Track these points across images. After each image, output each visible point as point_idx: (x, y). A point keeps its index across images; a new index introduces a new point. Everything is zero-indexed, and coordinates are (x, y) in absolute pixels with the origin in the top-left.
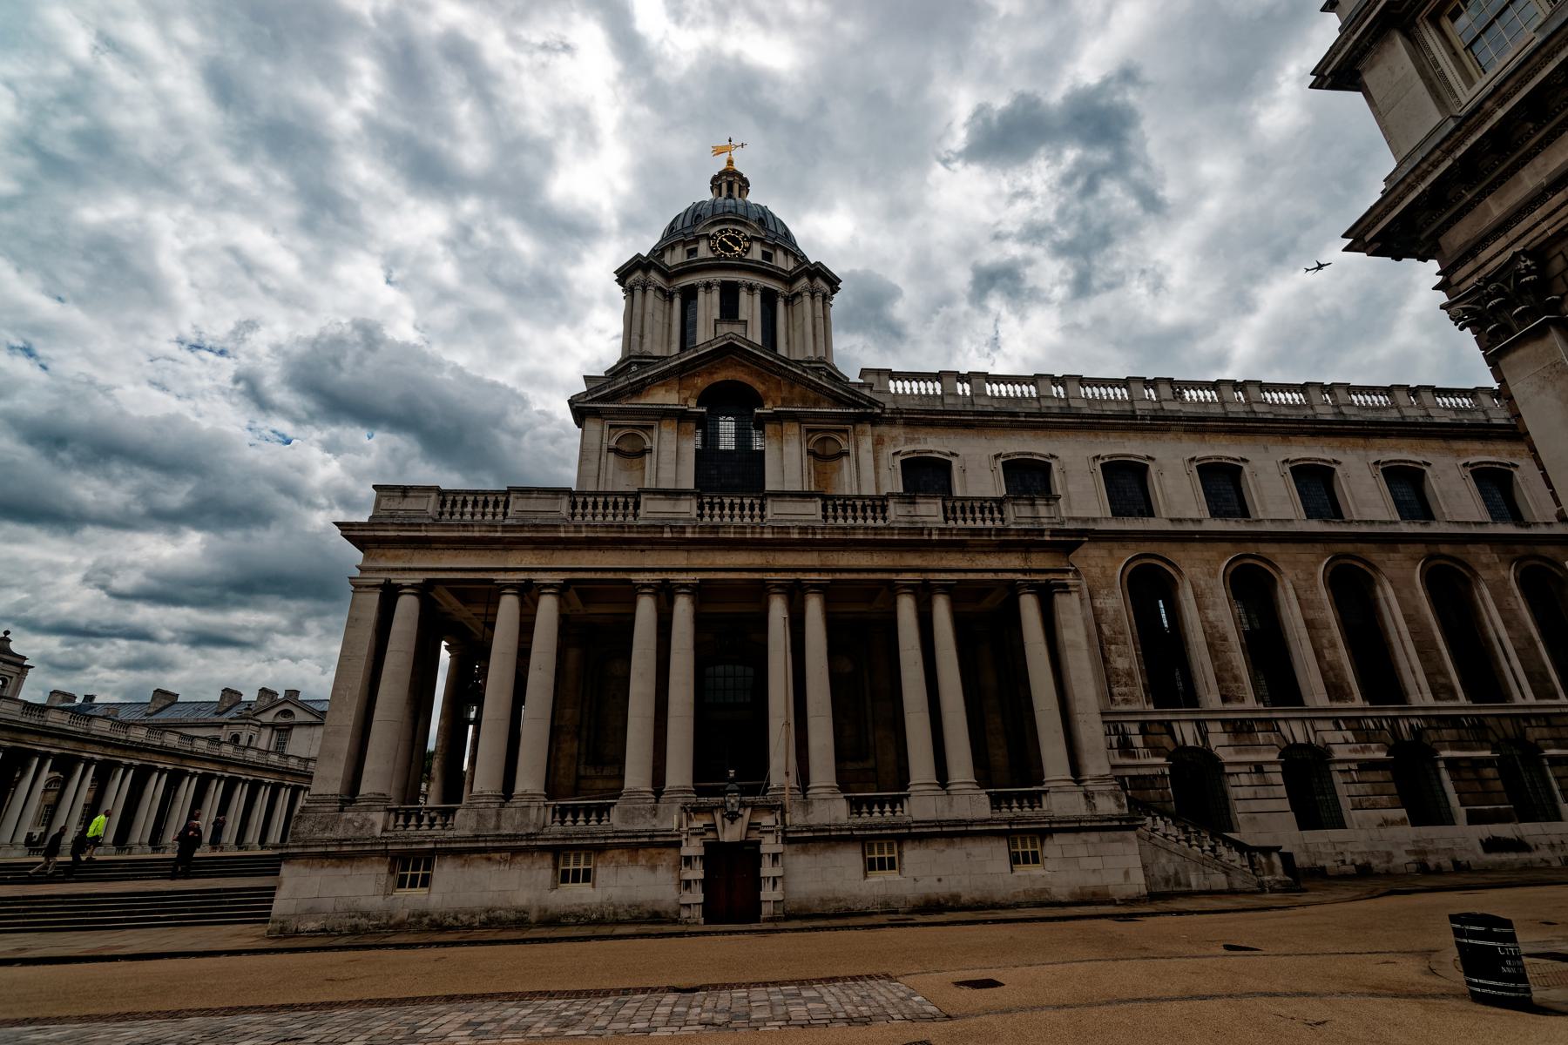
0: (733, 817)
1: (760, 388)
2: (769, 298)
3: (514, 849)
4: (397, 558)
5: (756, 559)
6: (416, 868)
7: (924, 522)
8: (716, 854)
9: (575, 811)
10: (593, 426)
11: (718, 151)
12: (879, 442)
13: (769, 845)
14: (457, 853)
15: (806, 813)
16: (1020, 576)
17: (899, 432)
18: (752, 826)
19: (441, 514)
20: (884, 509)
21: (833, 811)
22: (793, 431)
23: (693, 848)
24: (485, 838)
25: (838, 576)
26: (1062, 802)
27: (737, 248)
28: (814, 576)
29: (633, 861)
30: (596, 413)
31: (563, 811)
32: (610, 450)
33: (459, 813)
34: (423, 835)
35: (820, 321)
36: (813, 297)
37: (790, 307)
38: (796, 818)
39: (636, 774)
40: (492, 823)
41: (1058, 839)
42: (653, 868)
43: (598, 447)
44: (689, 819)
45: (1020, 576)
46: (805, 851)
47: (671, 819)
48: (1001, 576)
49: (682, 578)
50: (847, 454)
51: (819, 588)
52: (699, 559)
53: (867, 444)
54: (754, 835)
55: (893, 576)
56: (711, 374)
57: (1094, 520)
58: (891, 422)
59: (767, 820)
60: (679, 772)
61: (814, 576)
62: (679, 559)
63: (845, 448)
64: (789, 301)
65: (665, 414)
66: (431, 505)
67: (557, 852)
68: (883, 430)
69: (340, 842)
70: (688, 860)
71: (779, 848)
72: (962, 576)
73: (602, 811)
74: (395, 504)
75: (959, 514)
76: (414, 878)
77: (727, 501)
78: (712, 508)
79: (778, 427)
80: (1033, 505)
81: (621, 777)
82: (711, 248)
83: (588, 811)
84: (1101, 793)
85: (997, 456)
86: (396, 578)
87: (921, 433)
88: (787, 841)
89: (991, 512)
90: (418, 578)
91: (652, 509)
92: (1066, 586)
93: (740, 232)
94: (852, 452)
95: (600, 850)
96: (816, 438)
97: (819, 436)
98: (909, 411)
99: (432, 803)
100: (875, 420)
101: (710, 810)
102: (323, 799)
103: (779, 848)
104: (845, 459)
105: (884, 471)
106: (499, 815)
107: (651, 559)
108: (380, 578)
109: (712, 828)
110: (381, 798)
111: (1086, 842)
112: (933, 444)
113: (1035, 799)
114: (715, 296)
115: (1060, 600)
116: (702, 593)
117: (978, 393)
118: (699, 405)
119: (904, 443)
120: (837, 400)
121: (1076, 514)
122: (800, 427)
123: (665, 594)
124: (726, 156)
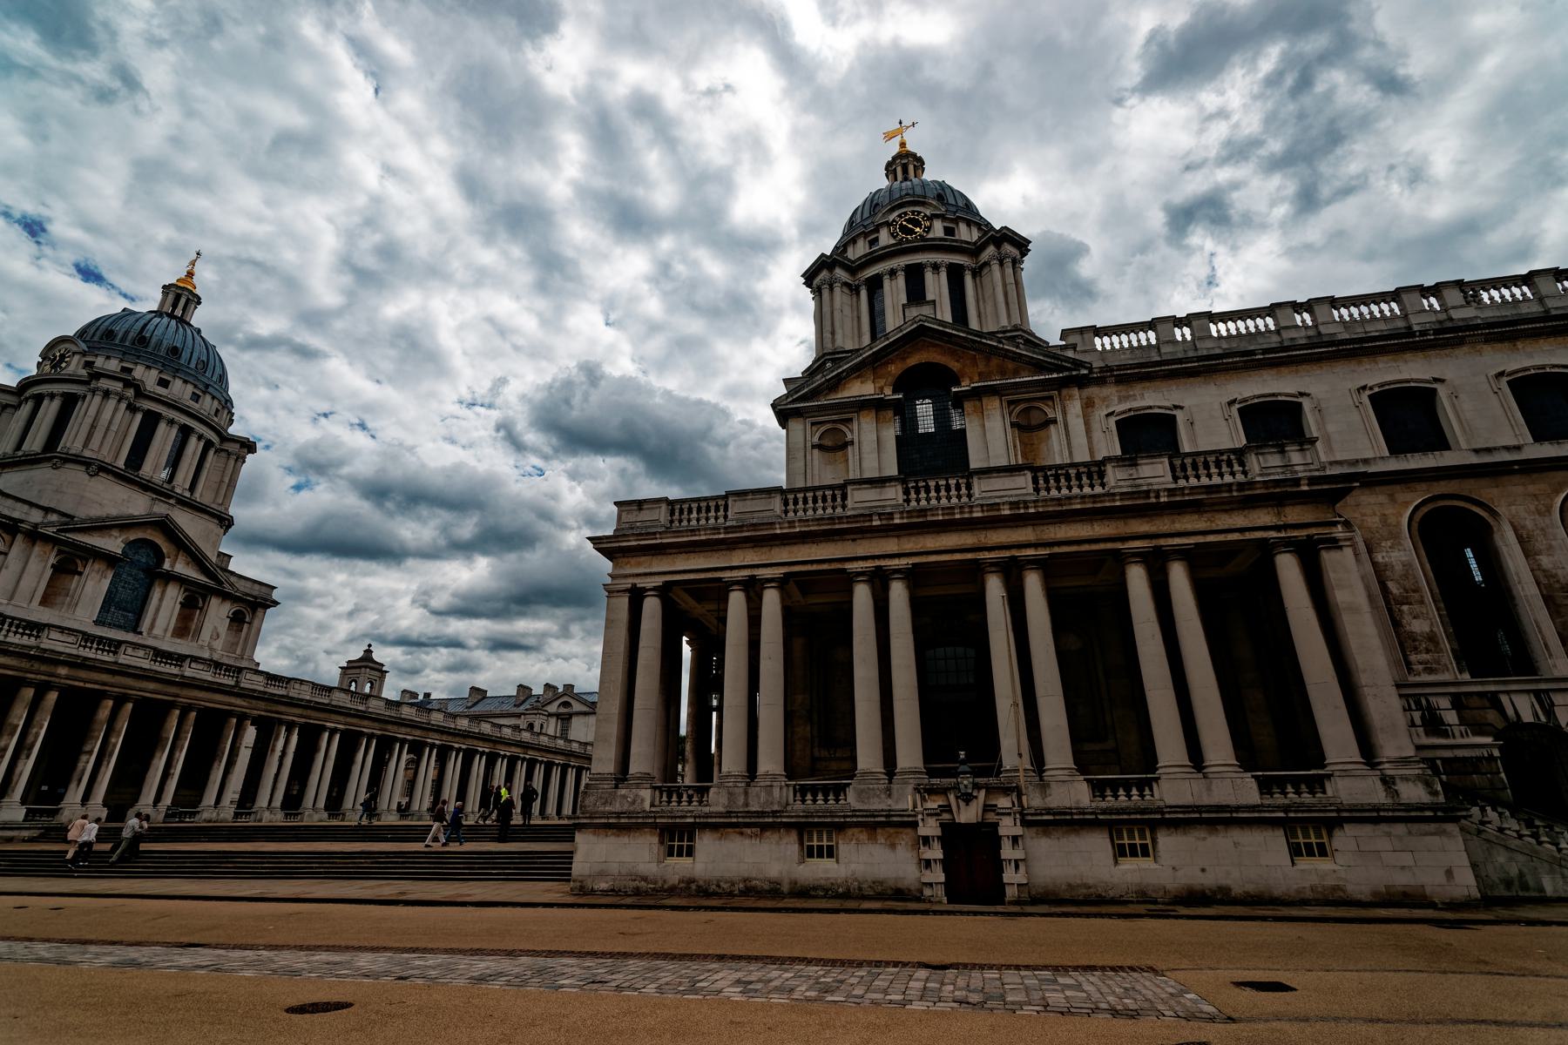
0: (968, 799)
1: (955, 366)
2: (955, 274)
3: (763, 824)
4: (639, 564)
5: (967, 539)
6: (681, 840)
7: (1151, 484)
8: (952, 834)
9: (814, 790)
10: (797, 425)
11: (889, 136)
12: (1088, 405)
13: (1008, 827)
14: (715, 827)
15: (1044, 794)
16: (1273, 534)
17: (1110, 391)
18: (987, 808)
19: (672, 522)
20: (1102, 475)
21: (1076, 794)
22: (994, 407)
23: (930, 828)
25: (1056, 550)
27: (918, 229)
28: (1030, 552)
29: (873, 838)
30: (798, 413)
31: (802, 791)
32: (813, 447)
33: (712, 790)
34: (686, 809)
35: (1012, 289)
36: (1001, 264)
37: (978, 279)
38: (1034, 800)
39: (868, 756)
40: (741, 800)
42: (893, 846)
43: (802, 445)
44: (923, 800)
45: (1273, 534)
46: (1047, 834)
47: (905, 800)
48: (1248, 536)
49: (895, 563)
50: (1054, 421)
51: (1037, 563)
52: (909, 544)
53: (1075, 408)
54: (991, 817)
55: (1119, 546)
56: (904, 359)
57: (1366, 461)
58: (1101, 382)
59: (1003, 802)
60: (909, 754)
61: (1030, 552)
62: (891, 546)
63: (1051, 415)
64: (977, 273)
65: (862, 405)
66: (662, 515)
67: (802, 829)
68: (1093, 391)
69: (618, 815)
70: (926, 840)
71: (1018, 831)
72: (1200, 539)
73: (839, 790)
74: (632, 518)
75: (1190, 471)
77: (932, 484)
78: (918, 493)
79: (978, 403)
80: (1282, 452)
81: (854, 759)
82: (892, 234)
83: (826, 790)
84: (1405, 779)
85: (1231, 403)
86: (642, 583)
87: (1137, 389)
88: (1026, 824)
89: (1230, 464)
91: (859, 499)
92: (1335, 540)
93: (919, 213)
94: (1060, 418)
95: (841, 828)
96: (1018, 409)
98: (1120, 367)
99: (688, 781)
100: (1082, 383)
101: (944, 791)
102: (601, 778)
103: (1018, 831)
104: (1052, 427)
105: (1097, 435)
106: (746, 793)
108: (627, 583)
109: (947, 808)
110: (647, 777)
111: (1389, 835)
112: (1151, 398)
113: (1317, 784)
114: (901, 281)
115: (1328, 558)
116: (914, 577)
117: (1202, 336)
118: (894, 392)
119: (1116, 402)
120: (1039, 367)
121: (1339, 458)
122: (1001, 401)
123: (880, 581)
124: (898, 138)
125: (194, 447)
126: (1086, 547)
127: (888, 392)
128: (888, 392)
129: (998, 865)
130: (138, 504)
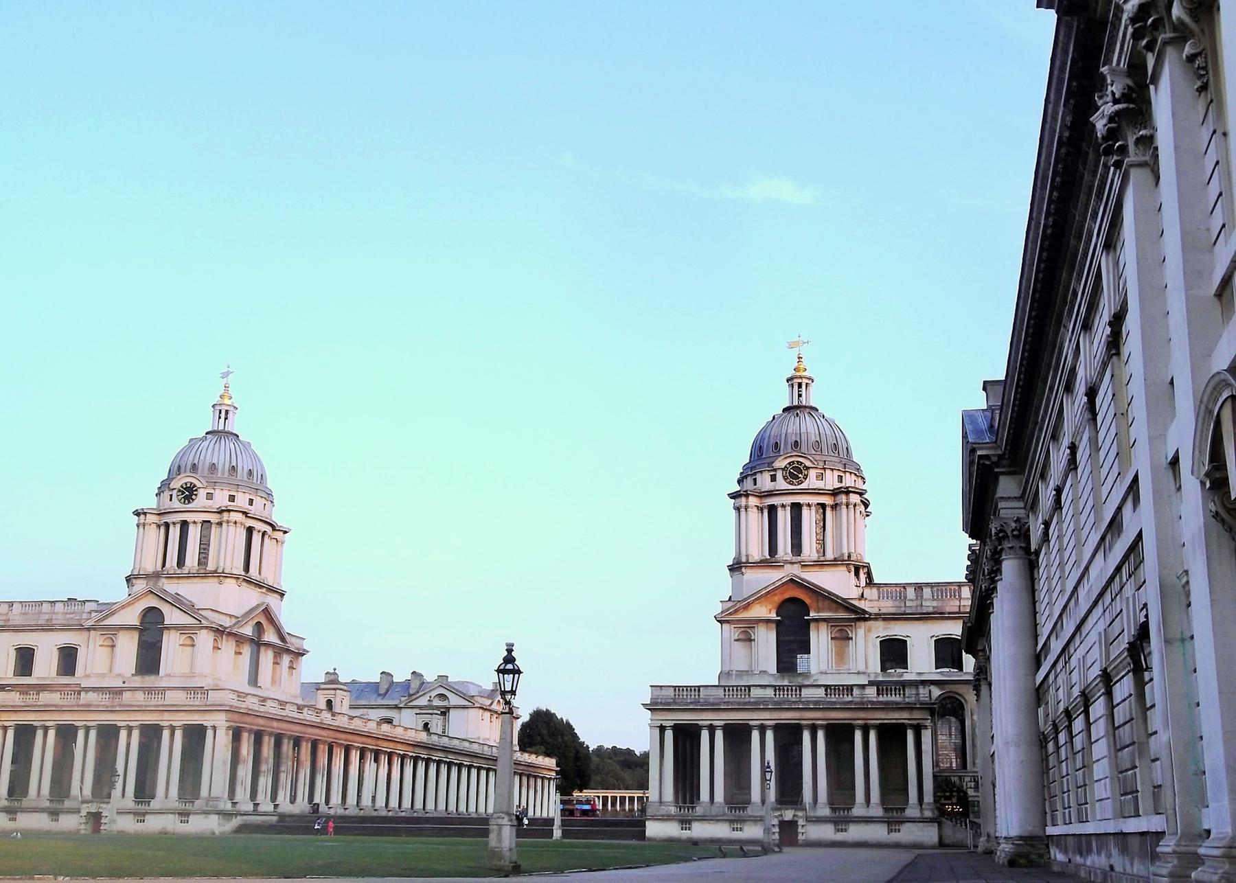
1: (807, 601)
4: (663, 715)
6: (686, 824)
7: (868, 697)
10: (726, 626)
15: (815, 812)
16: (906, 721)
17: (880, 624)
19: (675, 695)
20: (852, 690)
22: (823, 627)
24: (707, 816)
26: (912, 811)
27: (800, 475)
30: (728, 622)
36: (847, 506)
37: (834, 512)
40: (708, 812)
41: (908, 825)
45: (906, 721)
48: (899, 721)
52: (775, 715)
54: (796, 819)
56: (782, 594)
58: (876, 619)
62: (766, 715)
63: (850, 636)
64: (835, 507)
66: (671, 692)
69: (663, 816)
75: (885, 692)
76: (686, 828)
79: (817, 625)
80: (917, 688)
82: (784, 477)
84: (927, 809)
86: (665, 724)
89: (900, 691)
90: (672, 723)
91: (756, 693)
92: (926, 726)
93: (802, 463)
94: (854, 638)
95: (744, 821)
96: (835, 630)
97: (838, 628)
100: (865, 620)
104: (850, 641)
107: (755, 715)
108: (658, 723)
111: (917, 826)
112: (898, 630)
115: (923, 732)
116: (778, 728)
118: (777, 616)
122: (827, 625)
124: (795, 352)
125: (256, 538)
126: (841, 722)
127: (773, 616)
128: (773, 616)
129: (797, 833)
130: (253, 597)
